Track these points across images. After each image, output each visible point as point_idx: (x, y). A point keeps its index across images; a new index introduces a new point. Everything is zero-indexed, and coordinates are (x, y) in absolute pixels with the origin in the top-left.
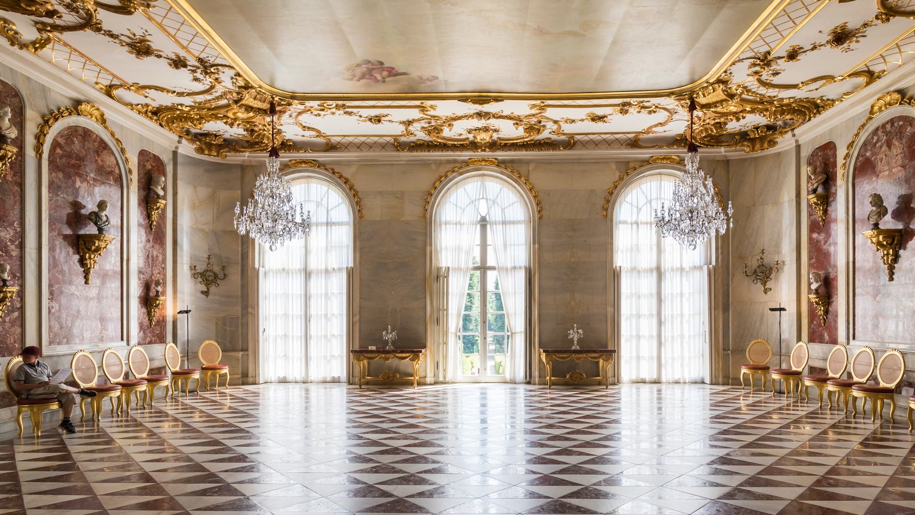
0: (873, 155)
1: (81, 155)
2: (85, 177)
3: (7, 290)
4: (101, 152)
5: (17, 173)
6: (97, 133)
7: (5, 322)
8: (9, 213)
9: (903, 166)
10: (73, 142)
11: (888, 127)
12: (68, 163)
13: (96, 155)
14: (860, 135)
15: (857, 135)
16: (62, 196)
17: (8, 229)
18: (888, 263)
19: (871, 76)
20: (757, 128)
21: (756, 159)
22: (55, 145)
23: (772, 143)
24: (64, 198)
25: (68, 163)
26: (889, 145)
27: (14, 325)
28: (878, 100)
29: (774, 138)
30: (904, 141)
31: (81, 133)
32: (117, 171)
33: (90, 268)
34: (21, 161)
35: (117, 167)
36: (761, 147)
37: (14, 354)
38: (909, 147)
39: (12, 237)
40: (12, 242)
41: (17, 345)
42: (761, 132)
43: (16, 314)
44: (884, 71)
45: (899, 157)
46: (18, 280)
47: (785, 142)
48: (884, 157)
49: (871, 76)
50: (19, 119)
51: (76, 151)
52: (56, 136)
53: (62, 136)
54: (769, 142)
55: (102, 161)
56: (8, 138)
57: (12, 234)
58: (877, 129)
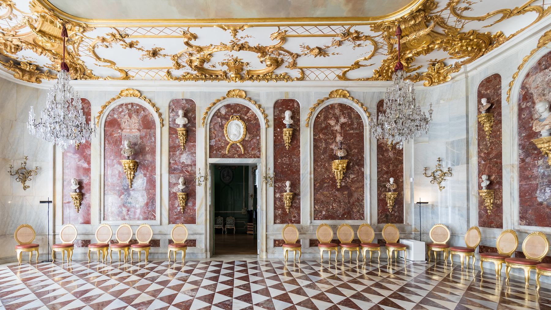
0: (119, 117)
9: (139, 130)
11: (130, 106)
14: (112, 103)
15: (110, 102)
18: (131, 179)
19: (127, 77)
20: (30, 64)
21: (18, 85)
23: (38, 80)
26: (130, 116)
28: (127, 90)
29: (41, 78)
30: (140, 117)
36: (30, 79)
38: (143, 121)
42: (32, 68)
44: (133, 77)
45: (137, 125)
47: (47, 84)
48: (127, 121)
49: (127, 77)
54: (37, 78)
58: (122, 105)
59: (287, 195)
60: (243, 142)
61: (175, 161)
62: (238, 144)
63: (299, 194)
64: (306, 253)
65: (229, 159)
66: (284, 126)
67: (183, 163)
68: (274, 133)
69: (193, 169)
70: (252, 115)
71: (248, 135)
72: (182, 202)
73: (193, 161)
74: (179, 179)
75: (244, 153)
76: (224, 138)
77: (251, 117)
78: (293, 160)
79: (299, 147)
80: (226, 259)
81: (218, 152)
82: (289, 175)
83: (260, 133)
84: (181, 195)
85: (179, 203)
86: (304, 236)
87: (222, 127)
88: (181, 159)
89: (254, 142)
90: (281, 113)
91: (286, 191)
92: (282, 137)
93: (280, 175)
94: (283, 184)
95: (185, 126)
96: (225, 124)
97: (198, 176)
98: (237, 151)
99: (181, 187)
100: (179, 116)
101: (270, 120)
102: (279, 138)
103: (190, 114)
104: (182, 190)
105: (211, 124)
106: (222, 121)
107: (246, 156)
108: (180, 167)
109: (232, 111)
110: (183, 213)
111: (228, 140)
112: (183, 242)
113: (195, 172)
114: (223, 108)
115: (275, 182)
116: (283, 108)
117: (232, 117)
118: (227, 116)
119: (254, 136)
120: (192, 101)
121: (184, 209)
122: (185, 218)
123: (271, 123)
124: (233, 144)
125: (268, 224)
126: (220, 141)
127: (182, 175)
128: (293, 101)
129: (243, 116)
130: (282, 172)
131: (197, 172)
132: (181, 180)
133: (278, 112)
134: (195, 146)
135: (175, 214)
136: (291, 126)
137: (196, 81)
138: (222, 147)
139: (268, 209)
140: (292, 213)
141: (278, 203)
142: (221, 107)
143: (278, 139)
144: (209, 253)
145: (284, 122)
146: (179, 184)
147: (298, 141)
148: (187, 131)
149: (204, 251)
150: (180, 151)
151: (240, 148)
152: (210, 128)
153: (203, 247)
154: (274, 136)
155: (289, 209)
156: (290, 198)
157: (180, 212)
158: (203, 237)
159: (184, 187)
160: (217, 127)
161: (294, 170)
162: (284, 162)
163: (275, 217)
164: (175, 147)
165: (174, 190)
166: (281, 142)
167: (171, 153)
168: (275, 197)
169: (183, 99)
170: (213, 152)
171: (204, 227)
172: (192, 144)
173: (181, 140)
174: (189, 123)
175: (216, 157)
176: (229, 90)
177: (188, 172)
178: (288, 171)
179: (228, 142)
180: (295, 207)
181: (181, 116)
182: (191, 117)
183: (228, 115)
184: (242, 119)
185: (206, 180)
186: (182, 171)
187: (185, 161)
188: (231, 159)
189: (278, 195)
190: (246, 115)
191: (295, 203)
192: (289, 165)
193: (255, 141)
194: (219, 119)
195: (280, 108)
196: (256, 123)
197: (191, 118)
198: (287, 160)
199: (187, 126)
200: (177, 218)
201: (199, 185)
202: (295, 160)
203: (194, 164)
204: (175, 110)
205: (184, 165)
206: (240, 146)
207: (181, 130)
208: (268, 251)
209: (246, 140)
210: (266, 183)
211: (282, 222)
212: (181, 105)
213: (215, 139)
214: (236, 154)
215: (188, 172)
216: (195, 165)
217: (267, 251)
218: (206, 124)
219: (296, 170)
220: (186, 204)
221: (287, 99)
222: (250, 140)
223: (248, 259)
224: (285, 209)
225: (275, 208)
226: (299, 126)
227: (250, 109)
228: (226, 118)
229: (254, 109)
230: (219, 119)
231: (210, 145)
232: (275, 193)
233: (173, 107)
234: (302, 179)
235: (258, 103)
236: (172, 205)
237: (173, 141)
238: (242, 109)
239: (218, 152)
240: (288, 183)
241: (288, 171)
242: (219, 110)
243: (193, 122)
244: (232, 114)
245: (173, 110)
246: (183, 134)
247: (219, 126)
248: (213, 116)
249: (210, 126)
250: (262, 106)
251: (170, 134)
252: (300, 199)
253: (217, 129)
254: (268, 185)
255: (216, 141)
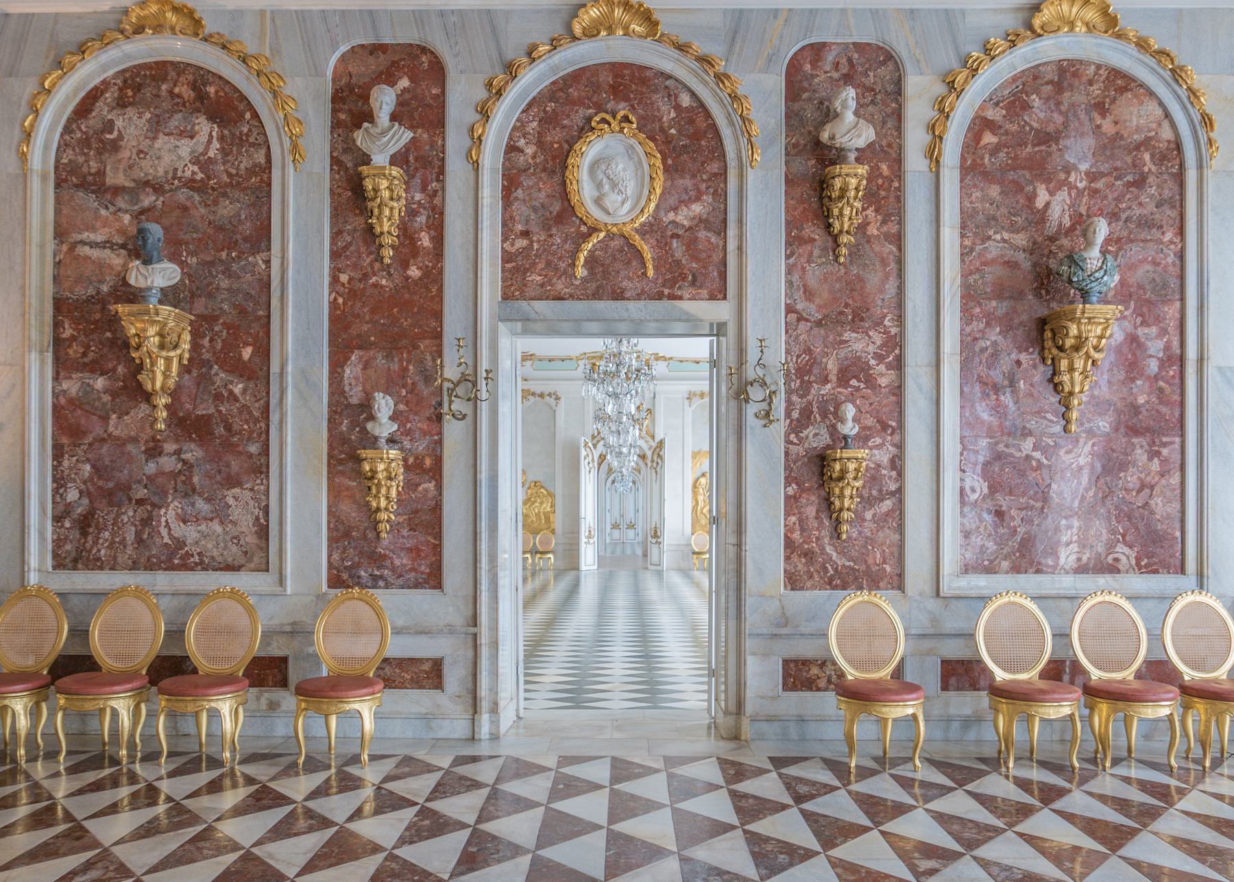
1: (1051, 129)
2: (1062, 176)
3: (844, 455)
4: (1113, 101)
5: (892, 214)
6: (1095, 58)
7: (864, 520)
8: (874, 301)
10: (1026, 107)
12: (1016, 158)
13: (1096, 115)
16: (998, 237)
17: (871, 333)
22: (981, 124)
24: (1004, 241)
25: (1016, 158)
27: (882, 527)
31: (1048, 77)
32: (1166, 134)
33: (1071, 393)
34: (898, 189)
35: (1166, 124)
37: (881, 584)
39: (880, 347)
40: (880, 358)
41: (888, 569)
43: (887, 504)
46: (892, 434)
50: (894, 105)
51: (1035, 125)
52: (981, 108)
53: (997, 104)
55: (1116, 123)
56: (850, 150)
57: (879, 343)
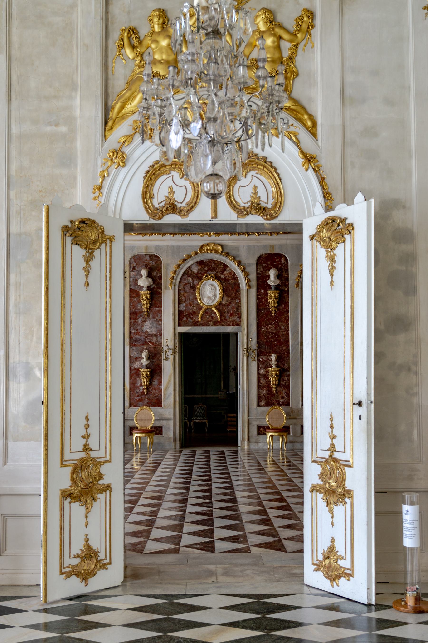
59: (273, 371)
60: (219, 306)
61: (137, 330)
62: (213, 309)
63: (288, 370)
64: (297, 442)
65: (202, 327)
66: (269, 287)
67: (147, 332)
68: (257, 295)
69: (159, 339)
70: (231, 273)
71: (225, 298)
72: (145, 380)
73: (159, 330)
74: (142, 352)
75: (221, 319)
76: (196, 302)
77: (228, 276)
78: (280, 328)
79: (288, 311)
80: (199, 451)
81: (189, 319)
82: (275, 346)
83: (240, 295)
84: (144, 372)
85: (143, 380)
86: (294, 421)
87: (193, 288)
88: (144, 328)
89: (233, 307)
90: (265, 271)
91: (271, 367)
92: (267, 300)
93: (264, 346)
94: (268, 357)
95: (149, 288)
96: (197, 285)
97: (164, 348)
98: (212, 317)
99: (144, 362)
100: (141, 276)
101: (251, 280)
102: (263, 300)
103: (155, 273)
104: (146, 365)
105: (181, 284)
106: (193, 281)
107: (223, 323)
108: (142, 338)
109: (206, 269)
110: (147, 394)
111: (201, 304)
112: (149, 428)
113: (161, 344)
114: (194, 265)
115: (258, 356)
116: (268, 264)
117: (206, 276)
118: (200, 275)
119: (232, 299)
120: (156, 256)
121: (147, 389)
122: (149, 400)
123: (254, 283)
124: (207, 309)
125: (250, 407)
126: (191, 305)
127: (145, 347)
128: (280, 256)
129: (219, 274)
130: (267, 343)
131: (164, 344)
132: (144, 354)
133: (262, 270)
134: (161, 311)
135: (137, 395)
136: (277, 288)
137: (163, 236)
138: (194, 312)
139: (250, 388)
140: (279, 393)
141: (262, 381)
142: (193, 264)
143: (262, 302)
144: (178, 443)
145: (269, 282)
146: (143, 358)
147: (287, 304)
148: (151, 294)
149: (172, 440)
150: (143, 318)
151: (215, 313)
152: (179, 290)
153: (172, 435)
154: (258, 298)
155: (276, 388)
156: (276, 374)
157: (143, 393)
158: (171, 423)
159: (148, 362)
160: (188, 289)
161: (282, 340)
162: (270, 330)
163: (259, 398)
164: (136, 313)
165: (136, 366)
166: (266, 306)
167: (132, 321)
168: (258, 373)
169: (146, 255)
170: (182, 319)
171: (172, 411)
172: (157, 309)
173: (144, 304)
174: (154, 283)
175: (186, 324)
176: (202, 244)
177: (152, 343)
178: (274, 341)
179: (201, 306)
180: (283, 385)
181: (144, 277)
182: (155, 276)
183: (201, 273)
184: (218, 278)
185: (175, 353)
186: (146, 342)
187: (148, 330)
188: (205, 327)
189: (262, 371)
190: (222, 273)
191: (284, 380)
192: (275, 334)
193: (233, 304)
194: (190, 278)
195: (264, 265)
196: (235, 283)
197: (155, 278)
198: (274, 328)
199: (152, 287)
200: (140, 400)
201: (167, 359)
202: (283, 327)
203: (160, 333)
204: (136, 268)
205: (148, 335)
206: (216, 311)
207: (144, 294)
208: (250, 440)
209: (223, 305)
210: (248, 357)
211: (267, 404)
212: (143, 262)
213: (185, 302)
214: (210, 321)
215: (152, 343)
216: (161, 335)
217: (249, 440)
218: (175, 285)
219: (284, 339)
220: (151, 383)
221: (272, 253)
222: (227, 303)
223: (227, 450)
224: (271, 388)
225: (259, 387)
226: (287, 286)
227: (228, 267)
228: (199, 277)
229: (233, 266)
230: (190, 278)
231: (179, 311)
232: (258, 368)
233: (135, 264)
234: (292, 351)
235: (238, 259)
236: (133, 384)
237: (133, 306)
238: (218, 266)
239: (189, 319)
240: (273, 357)
241: (274, 341)
242: (190, 267)
243: (158, 283)
244: (206, 273)
245: (134, 268)
246: (147, 298)
247: (191, 287)
248: (183, 275)
249: (179, 287)
250: (242, 262)
251: (130, 297)
252: (289, 376)
253: (187, 290)
254: (250, 359)
255: (186, 305)
